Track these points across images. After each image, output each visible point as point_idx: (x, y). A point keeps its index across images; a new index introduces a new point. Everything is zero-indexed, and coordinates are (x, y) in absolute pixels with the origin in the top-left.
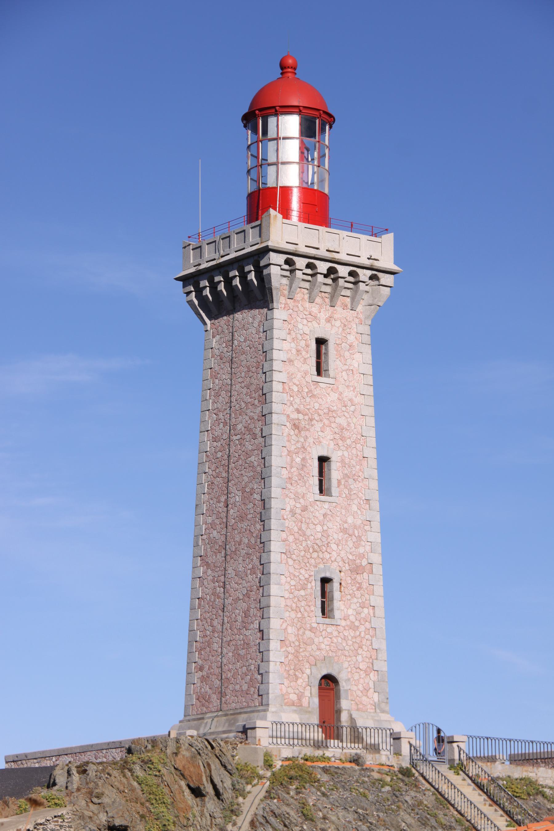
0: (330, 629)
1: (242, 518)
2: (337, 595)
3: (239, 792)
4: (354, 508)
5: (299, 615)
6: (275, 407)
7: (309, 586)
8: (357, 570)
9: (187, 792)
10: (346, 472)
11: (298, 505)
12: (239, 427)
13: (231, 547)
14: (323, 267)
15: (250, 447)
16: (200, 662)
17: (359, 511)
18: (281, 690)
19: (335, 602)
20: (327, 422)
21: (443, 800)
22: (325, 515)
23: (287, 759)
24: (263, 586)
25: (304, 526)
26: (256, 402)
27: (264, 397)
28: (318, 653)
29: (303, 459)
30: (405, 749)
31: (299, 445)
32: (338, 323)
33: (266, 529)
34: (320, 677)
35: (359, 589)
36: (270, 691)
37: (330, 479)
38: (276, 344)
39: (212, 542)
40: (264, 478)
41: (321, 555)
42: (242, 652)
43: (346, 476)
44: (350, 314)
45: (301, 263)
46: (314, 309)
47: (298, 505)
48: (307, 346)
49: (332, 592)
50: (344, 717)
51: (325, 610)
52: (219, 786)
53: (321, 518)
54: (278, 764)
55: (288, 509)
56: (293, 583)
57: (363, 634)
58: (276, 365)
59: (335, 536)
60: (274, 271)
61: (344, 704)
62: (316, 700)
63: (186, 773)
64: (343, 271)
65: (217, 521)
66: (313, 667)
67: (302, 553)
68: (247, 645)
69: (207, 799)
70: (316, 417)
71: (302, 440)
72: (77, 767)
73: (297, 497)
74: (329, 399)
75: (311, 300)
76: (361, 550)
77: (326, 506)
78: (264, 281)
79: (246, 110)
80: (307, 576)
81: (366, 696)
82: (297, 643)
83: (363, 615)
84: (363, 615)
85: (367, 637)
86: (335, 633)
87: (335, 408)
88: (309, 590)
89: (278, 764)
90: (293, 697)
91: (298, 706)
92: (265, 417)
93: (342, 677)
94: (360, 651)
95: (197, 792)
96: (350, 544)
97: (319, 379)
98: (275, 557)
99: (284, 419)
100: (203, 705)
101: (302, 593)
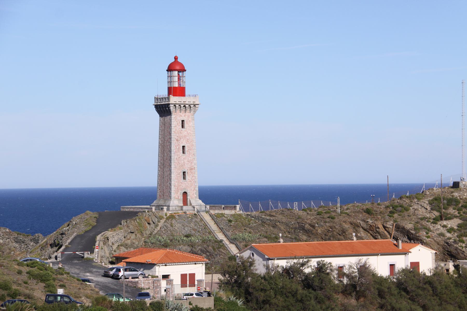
1: (167, 159)
2: (187, 175)
3: (159, 222)
8: (191, 169)
9: (147, 224)
13: (165, 165)
14: (182, 106)
21: (202, 220)
24: (170, 174)
27: (170, 134)
30: (196, 210)
33: (171, 163)
38: (172, 123)
39: (161, 163)
40: (170, 151)
44: (189, 114)
46: (181, 114)
50: (188, 200)
51: (184, 178)
54: (168, 215)
60: (171, 108)
61: (188, 197)
64: (187, 106)
68: (168, 186)
73: (177, 155)
75: (180, 112)
78: (170, 110)
89: (168, 215)
91: (178, 199)
93: (188, 192)
95: (149, 224)
98: (172, 169)
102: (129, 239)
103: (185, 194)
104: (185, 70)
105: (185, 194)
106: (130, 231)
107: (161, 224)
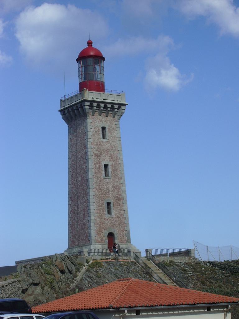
0: (110, 218)
1: (81, 185)
2: (112, 207)
3: (78, 270)
4: (117, 180)
5: (100, 215)
6: (89, 150)
7: (103, 205)
9: (59, 273)
10: (114, 169)
11: (98, 180)
12: (79, 156)
15: (83, 163)
16: (72, 231)
17: (118, 181)
18: (95, 238)
19: (112, 210)
20: (106, 153)
22: (107, 183)
23: (94, 260)
25: (100, 187)
26: (84, 148)
27: (86, 147)
28: (107, 226)
29: (100, 166)
31: (98, 161)
32: (109, 122)
34: (108, 233)
35: (119, 205)
36: (92, 239)
37: (108, 171)
38: (89, 130)
41: (107, 195)
42: (83, 227)
43: (113, 170)
45: (95, 104)
46: (101, 118)
47: (98, 180)
48: (99, 130)
49: (111, 207)
51: (109, 212)
52: (70, 269)
53: (106, 184)
54: (91, 262)
55: (95, 181)
56: (98, 205)
57: (121, 219)
58: (89, 137)
59: (111, 189)
62: (107, 241)
63: (59, 266)
64: (109, 106)
65: (74, 187)
66: (105, 231)
67: (101, 195)
69: (66, 274)
70: (103, 152)
71: (99, 160)
72: (23, 267)
73: (98, 179)
74: (107, 146)
76: (120, 193)
77: (107, 180)
79: (77, 57)
80: (102, 202)
81: (123, 238)
82: (100, 224)
83: (121, 213)
84: (121, 213)
85: (123, 220)
86: (112, 220)
87: (109, 149)
88: (103, 207)
89: (91, 262)
90: (99, 240)
93: (115, 233)
94: (121, 225)
95: (63, 272)
96: (116, 191)
97: (103, 140)
99: (92, 153)
100: (73, 244)
101: (101, 208)
102: (31, 295)
103: (111, 236)
105: (111, 236)
106: (31, 281)
107: (80, 275)
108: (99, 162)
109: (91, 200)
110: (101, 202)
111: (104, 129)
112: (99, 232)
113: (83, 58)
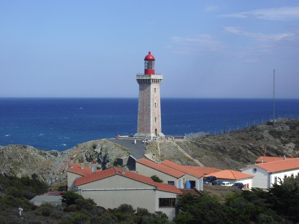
27: (149, 96)
51: (156, 121)
61: (157, 132)
64: (158, 80)
68: (147, 126)
92: (149, 99)
93: (157, 129)
103: (156, 130)
104: (155, 60)
108: (153, 102)
109: (151, 117)
110: (154, 117)
111: (155, 89)
112: (153, 128)
113: (146, 59)
